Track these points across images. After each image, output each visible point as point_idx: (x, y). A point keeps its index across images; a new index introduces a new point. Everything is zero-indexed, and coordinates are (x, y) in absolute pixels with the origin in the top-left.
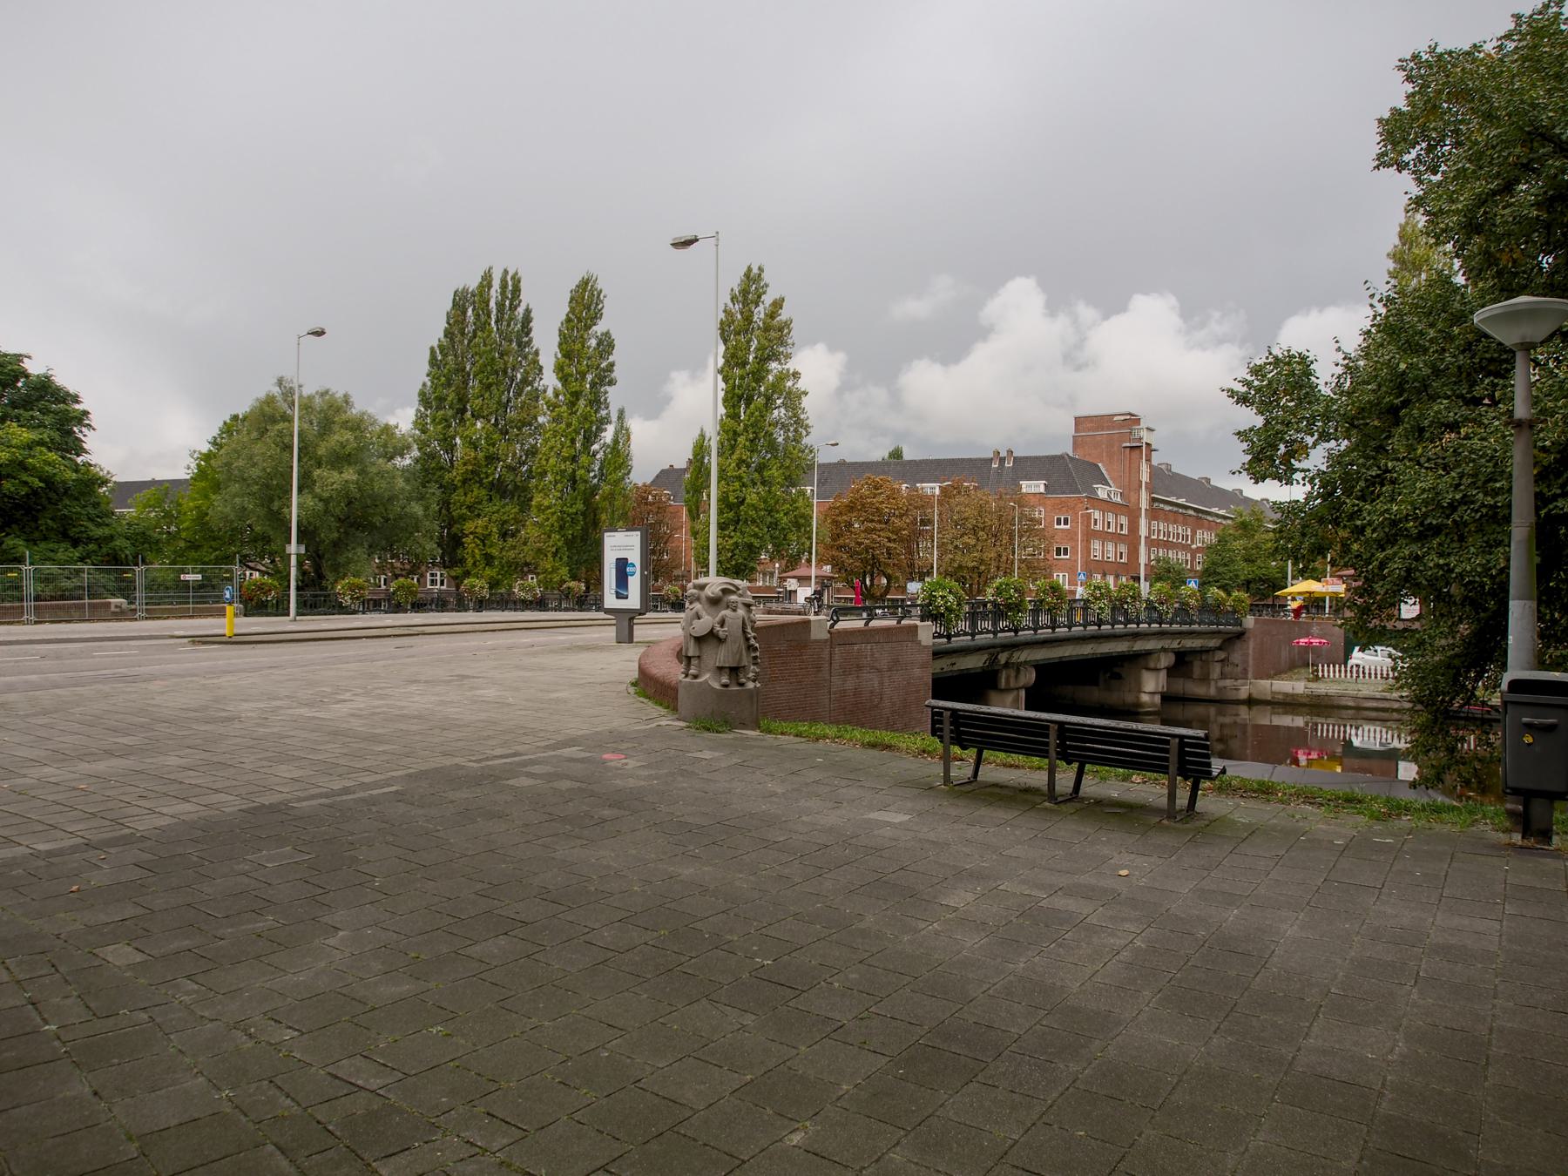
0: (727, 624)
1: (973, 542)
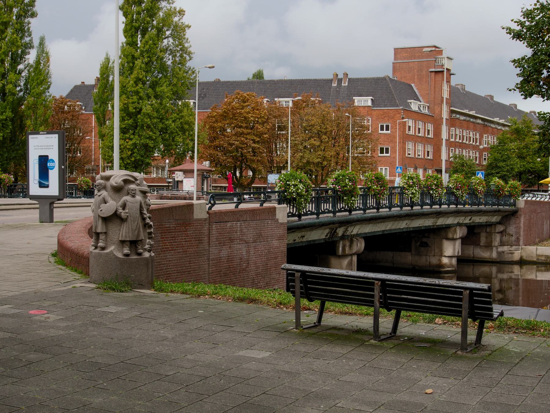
0: (127, 207)
1: (317, 143)
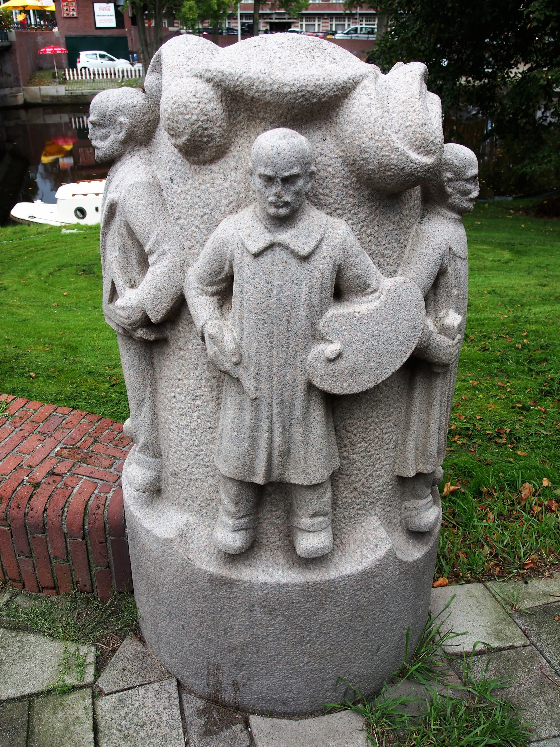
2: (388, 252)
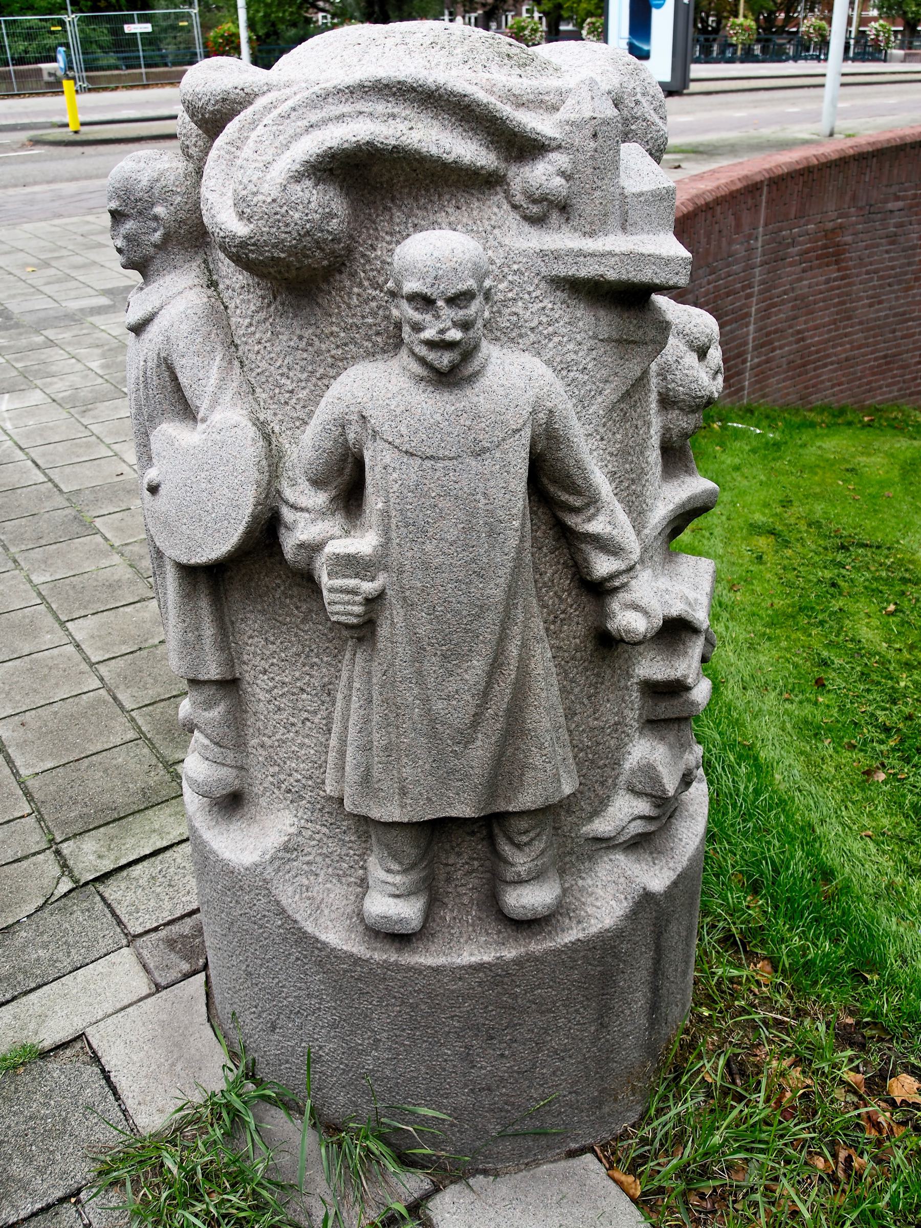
0: (374, 502)
2: (288, 382)
